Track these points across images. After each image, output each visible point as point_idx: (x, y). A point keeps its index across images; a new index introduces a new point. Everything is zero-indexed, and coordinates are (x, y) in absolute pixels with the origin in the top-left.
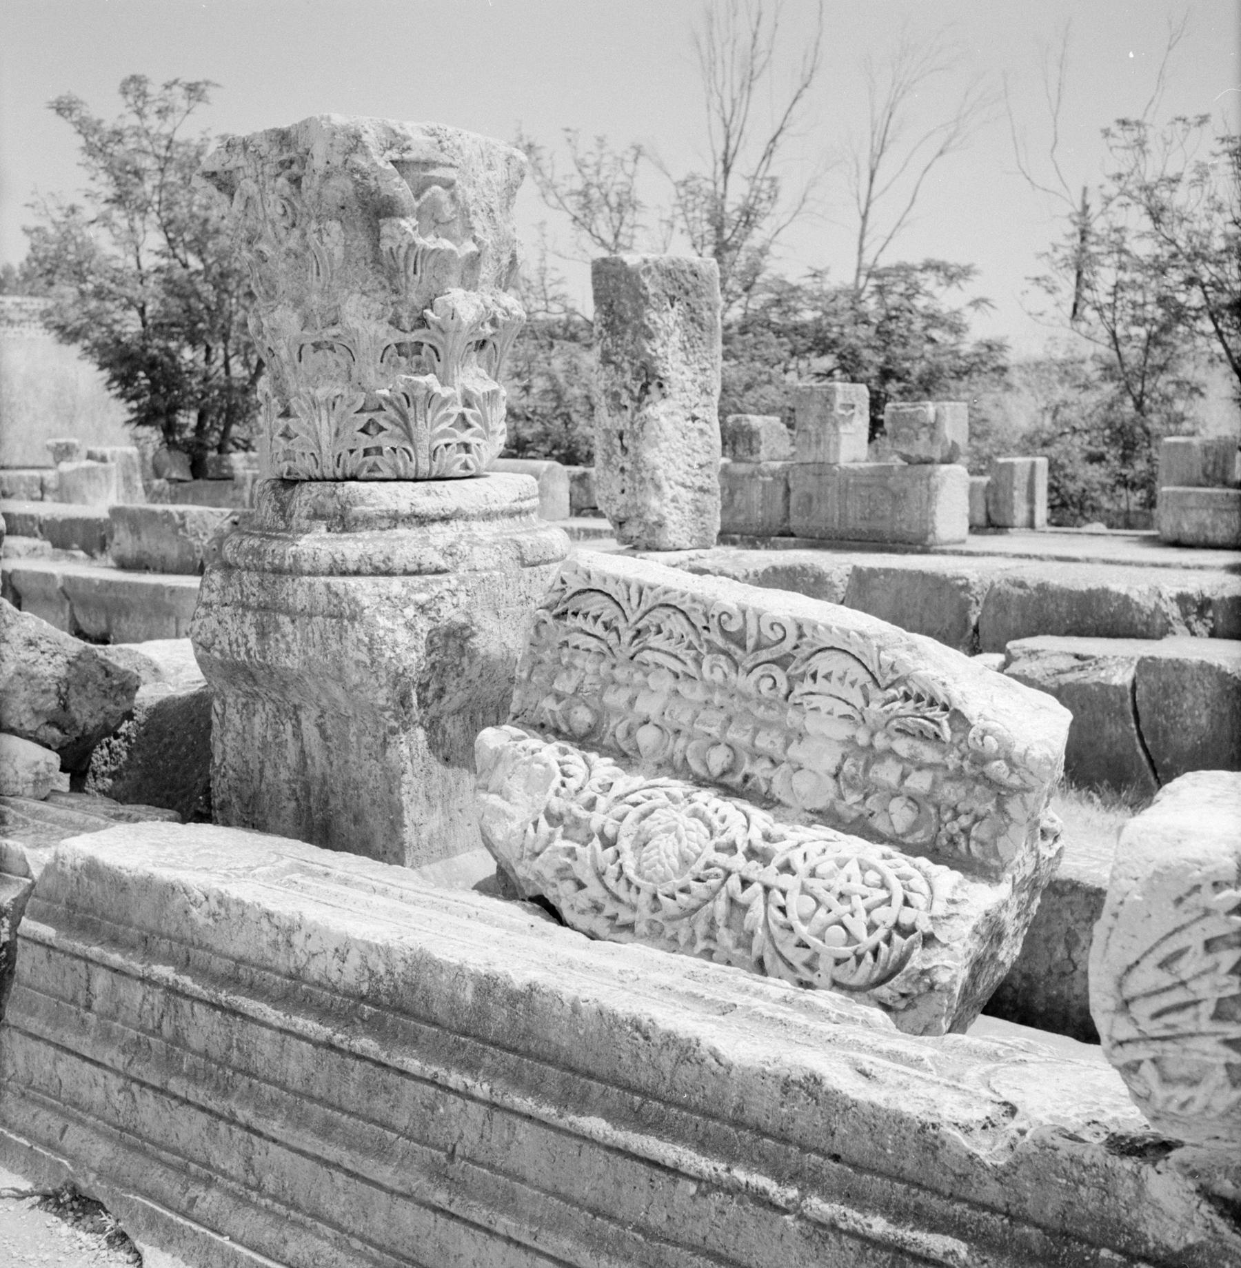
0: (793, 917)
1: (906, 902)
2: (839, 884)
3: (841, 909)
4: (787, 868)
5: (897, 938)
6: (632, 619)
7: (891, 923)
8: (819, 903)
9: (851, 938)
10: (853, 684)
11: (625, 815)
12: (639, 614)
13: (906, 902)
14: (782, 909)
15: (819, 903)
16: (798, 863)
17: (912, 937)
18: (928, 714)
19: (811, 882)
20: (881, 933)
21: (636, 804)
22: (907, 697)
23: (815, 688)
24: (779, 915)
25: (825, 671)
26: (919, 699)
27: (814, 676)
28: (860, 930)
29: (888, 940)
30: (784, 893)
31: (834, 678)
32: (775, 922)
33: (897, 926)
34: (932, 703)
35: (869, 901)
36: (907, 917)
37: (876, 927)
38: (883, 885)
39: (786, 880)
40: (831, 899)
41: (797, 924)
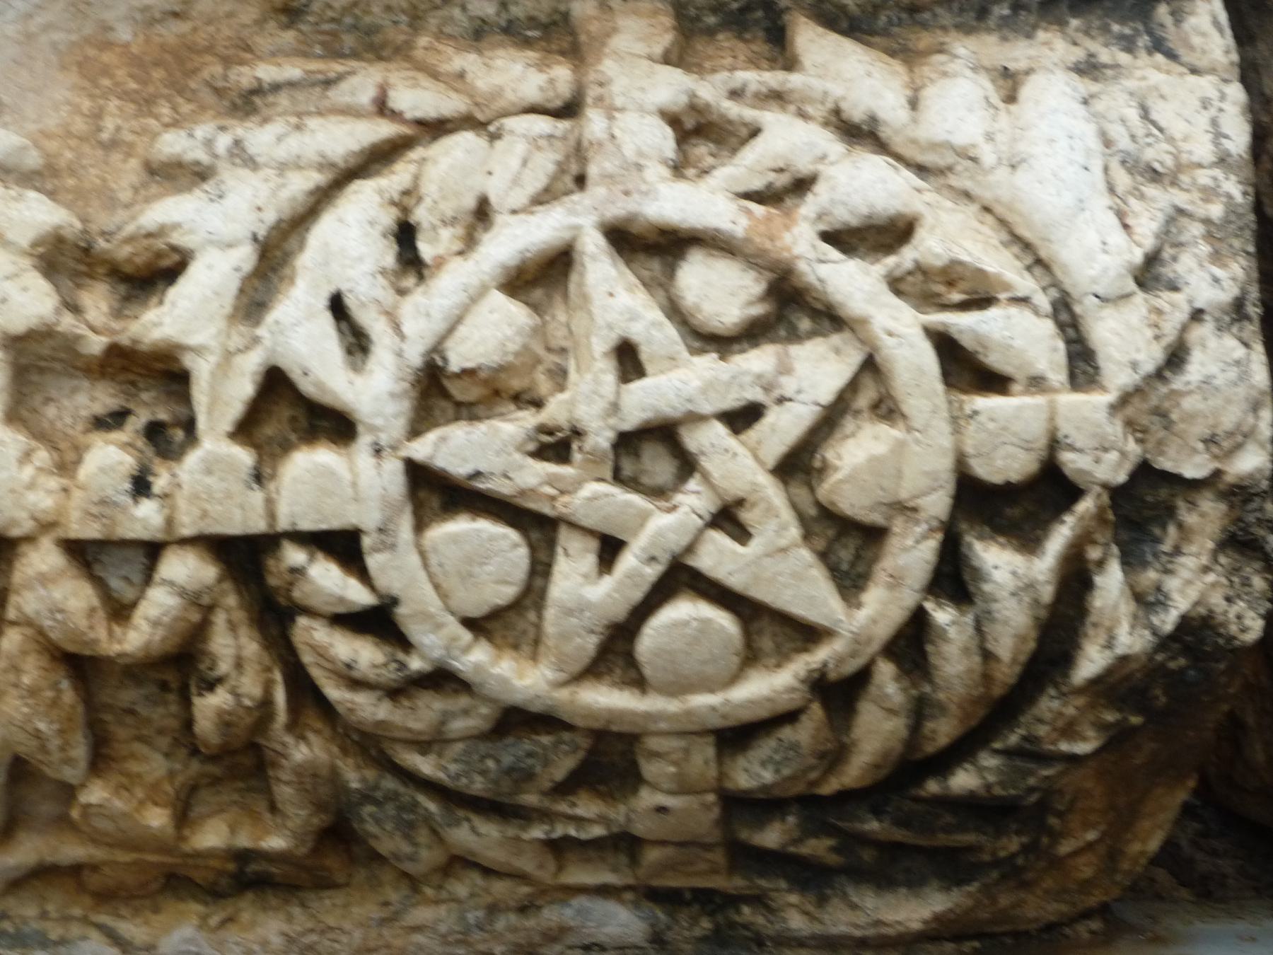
0: (436, 638)
2: (591, 400)
3: (661, 526)
5: (997, 562)
7: (938, 503)
8: (538, 527)
13: (965, 369)
14: (379, 621)
15: (538, 527)
16: (321, 365)
17: (1060, 537)
19: (457, 448)
24: (364, 653)
28: (802, 586)
29: (953, 578)
30: (344, 546)
36: (1003, 438)
37: (871, 536)
38: (791, 307)
40: (592, 496)
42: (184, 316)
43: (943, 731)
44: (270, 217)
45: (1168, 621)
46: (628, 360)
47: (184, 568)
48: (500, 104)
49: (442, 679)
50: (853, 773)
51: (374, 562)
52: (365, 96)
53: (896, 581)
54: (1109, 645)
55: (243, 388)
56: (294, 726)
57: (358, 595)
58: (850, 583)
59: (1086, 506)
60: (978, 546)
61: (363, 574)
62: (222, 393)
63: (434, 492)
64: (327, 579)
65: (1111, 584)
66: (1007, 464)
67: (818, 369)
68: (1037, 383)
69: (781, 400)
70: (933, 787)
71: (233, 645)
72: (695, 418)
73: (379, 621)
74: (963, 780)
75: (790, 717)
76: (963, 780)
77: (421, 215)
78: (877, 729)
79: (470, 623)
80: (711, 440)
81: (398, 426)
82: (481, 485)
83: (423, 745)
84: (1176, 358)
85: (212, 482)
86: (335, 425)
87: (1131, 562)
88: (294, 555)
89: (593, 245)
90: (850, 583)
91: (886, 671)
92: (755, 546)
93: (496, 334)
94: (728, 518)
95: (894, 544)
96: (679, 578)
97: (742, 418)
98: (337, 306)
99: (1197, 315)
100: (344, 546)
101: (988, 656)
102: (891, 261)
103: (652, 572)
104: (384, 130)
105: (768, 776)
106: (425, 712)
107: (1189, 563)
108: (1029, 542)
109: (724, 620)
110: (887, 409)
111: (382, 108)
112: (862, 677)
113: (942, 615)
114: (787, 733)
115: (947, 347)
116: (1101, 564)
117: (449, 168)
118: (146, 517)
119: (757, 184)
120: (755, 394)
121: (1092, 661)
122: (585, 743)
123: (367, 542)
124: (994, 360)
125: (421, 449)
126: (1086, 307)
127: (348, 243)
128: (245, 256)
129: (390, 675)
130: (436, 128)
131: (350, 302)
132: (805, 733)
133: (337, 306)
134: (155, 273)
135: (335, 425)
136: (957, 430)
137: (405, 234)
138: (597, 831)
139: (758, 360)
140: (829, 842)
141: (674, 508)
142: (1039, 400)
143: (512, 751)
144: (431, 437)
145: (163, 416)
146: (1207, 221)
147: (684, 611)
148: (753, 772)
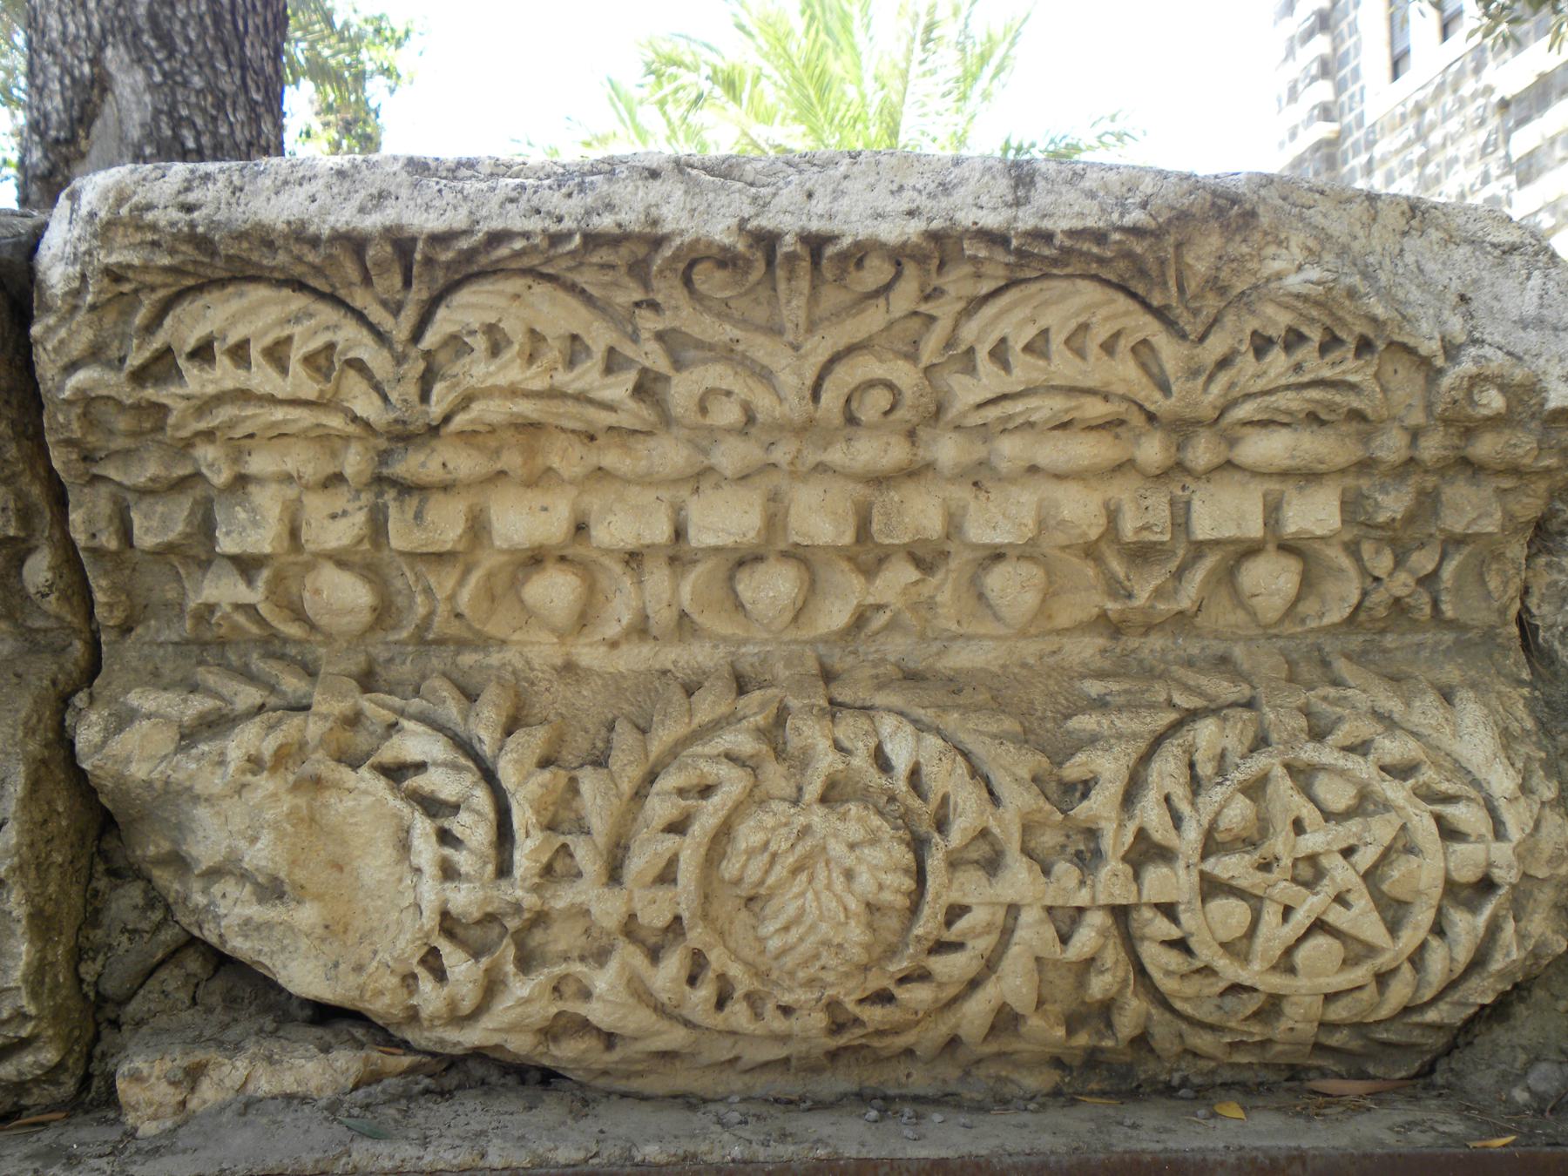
1: (1449, 833)
4: (1146, 852)
6: (400, 330)
7: (1437, 892)
9: (1356, 951)
10: (1109, 347)
11: (673, 862)
12: (409, 315)
13: (1449, 833)
14: (1181, 945)
15: (1255, 901)
18: (1327, 373)
20: (1423, 917)
21: (678, 827)
22: (1261, 345)
23: (1014, 383)
24: (1174, 959)
25: (1030, 332)
26: (1294, 339)
27: (1000, 354)
30: (1168, 910)
31: (1057, 342)
32: (1168, 973)
33: (1451, 888)
34: (1331, 343)
35: (1365, 858)
36: (1467, 861)
39: (1159, 882)
41: (1222, 963)
42: (1101, 806)
43: (1428, 995)
44: (1134, 756)
45: (1530, 944)
46: (1298, 827)
47: (1097, 919)
48: (1220, 702)
49: (1208, 971)
50: (1384, 1012)
51: (1184, 918)
52: (1162, 697)
53: (1415, 929)
54: (1508, 955)
55: (1129, 838)
56: (1135, 994)
57: (1175, 933)
58: (1393, 928)
59: (1502, 892)
60: (1452, 911)
61: (1175, 920)
62: (1115, 840)
63: (1211, 887)
64: (1163, 927)
65: (1509, 927)
66: (1467, 875)
67: (1381, 831)
68: (1481, 838)
69: (1366, 844)
70: (1416, 1018)
71: (1113, 955)
72: (1328, 852)
73: (1181, 945)
74: (1431, 1016)
75: (1360, 988)
76: (1431, 1016)
77: (1198, 757)
78: (1399, 992)
79: (1223, 945)
80: (1334, 863)
81: (1196, 858)
82: (1234, 883)
83: (1186, 999)
84: (1537, 826)
85: (1112, 883)
86: (1165, 855)
87: (1517, 919)
88: (1147, 913)
89: (1279, 771)
90: (1393, 928)
91: (1406, 967)
92: (1355, 911)
93: (1238, 813)
94: (1341, 899)
95: (1416, 909)
96: (1319, 926)
97: (1348, 852)
98: (1167, 799)
99: (1543, 804)
100: (1168, 910)
101: (1452, 960)
102: (1411, 782)
103: (1308, 923)
104: (1173, 716)
105: (1344, 1014)
106: (1191, 987)
107: (1537, 918)
108: (1473, 908)
109: (1336, 945)
110: (1411, 850)
111: (1171, 705)
112: (1394, 971)
113: (1435, 942)
114: (1357, 995)
115: (1439, 819)
116: (1505, 917)
117: (1206, 733)
118: (1082, 898)
119: (1348, 743)
120: (1352, 841)
121: (1497, 963)
122: (1263, 997)
123: (1182, 907)
124: (1463, 827)
125: (1208, 866)
126: (1502, 804)
127: (1166, 772)
128: (1124, 775)
129: (1185, 968)
130: (1192, 715)
131: (1174, 798)
132: (1364, 995)
133: (1167, 799)
134: (1085, 787)
135: (1165, 855)
136: (1446, 859)
137: (1192, 766)
138: (1257, 1038)
139: (1354, 825)
140: (1360, 1042)
141: (1317, 894)
142: (1481, 846)
143: (1230, 1002)
144: (1212, 860)
145: (1082, 847)
146: (1541, 760)
147: (1321, 941)
148: (1338, 1012)
